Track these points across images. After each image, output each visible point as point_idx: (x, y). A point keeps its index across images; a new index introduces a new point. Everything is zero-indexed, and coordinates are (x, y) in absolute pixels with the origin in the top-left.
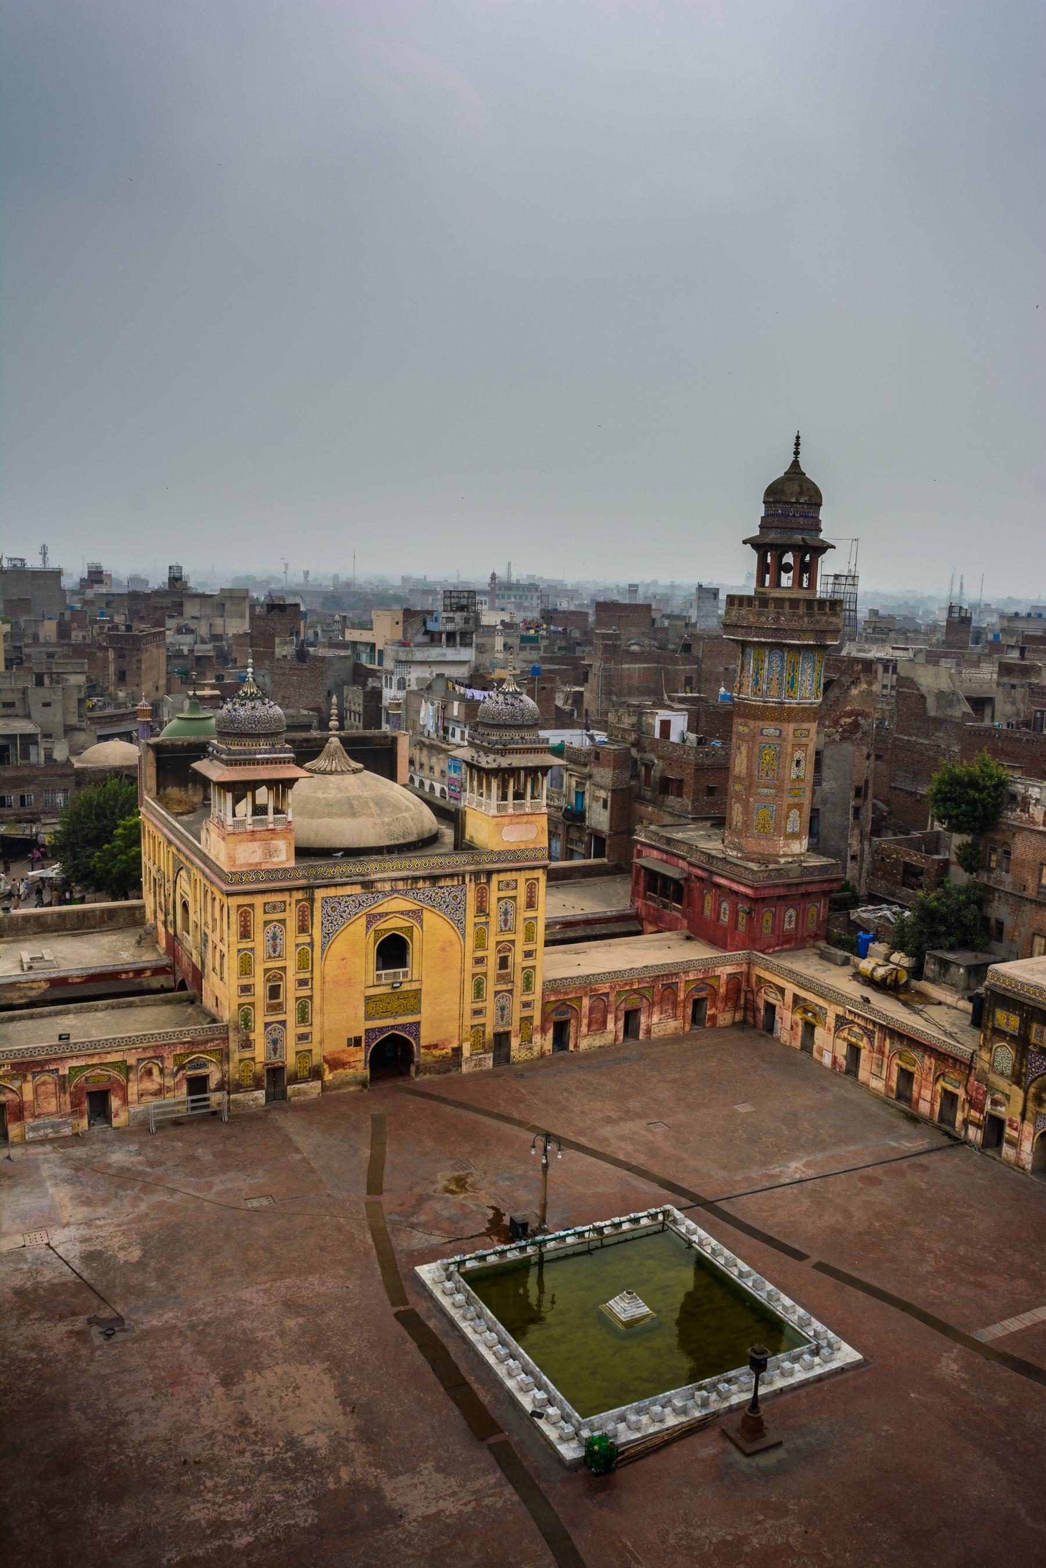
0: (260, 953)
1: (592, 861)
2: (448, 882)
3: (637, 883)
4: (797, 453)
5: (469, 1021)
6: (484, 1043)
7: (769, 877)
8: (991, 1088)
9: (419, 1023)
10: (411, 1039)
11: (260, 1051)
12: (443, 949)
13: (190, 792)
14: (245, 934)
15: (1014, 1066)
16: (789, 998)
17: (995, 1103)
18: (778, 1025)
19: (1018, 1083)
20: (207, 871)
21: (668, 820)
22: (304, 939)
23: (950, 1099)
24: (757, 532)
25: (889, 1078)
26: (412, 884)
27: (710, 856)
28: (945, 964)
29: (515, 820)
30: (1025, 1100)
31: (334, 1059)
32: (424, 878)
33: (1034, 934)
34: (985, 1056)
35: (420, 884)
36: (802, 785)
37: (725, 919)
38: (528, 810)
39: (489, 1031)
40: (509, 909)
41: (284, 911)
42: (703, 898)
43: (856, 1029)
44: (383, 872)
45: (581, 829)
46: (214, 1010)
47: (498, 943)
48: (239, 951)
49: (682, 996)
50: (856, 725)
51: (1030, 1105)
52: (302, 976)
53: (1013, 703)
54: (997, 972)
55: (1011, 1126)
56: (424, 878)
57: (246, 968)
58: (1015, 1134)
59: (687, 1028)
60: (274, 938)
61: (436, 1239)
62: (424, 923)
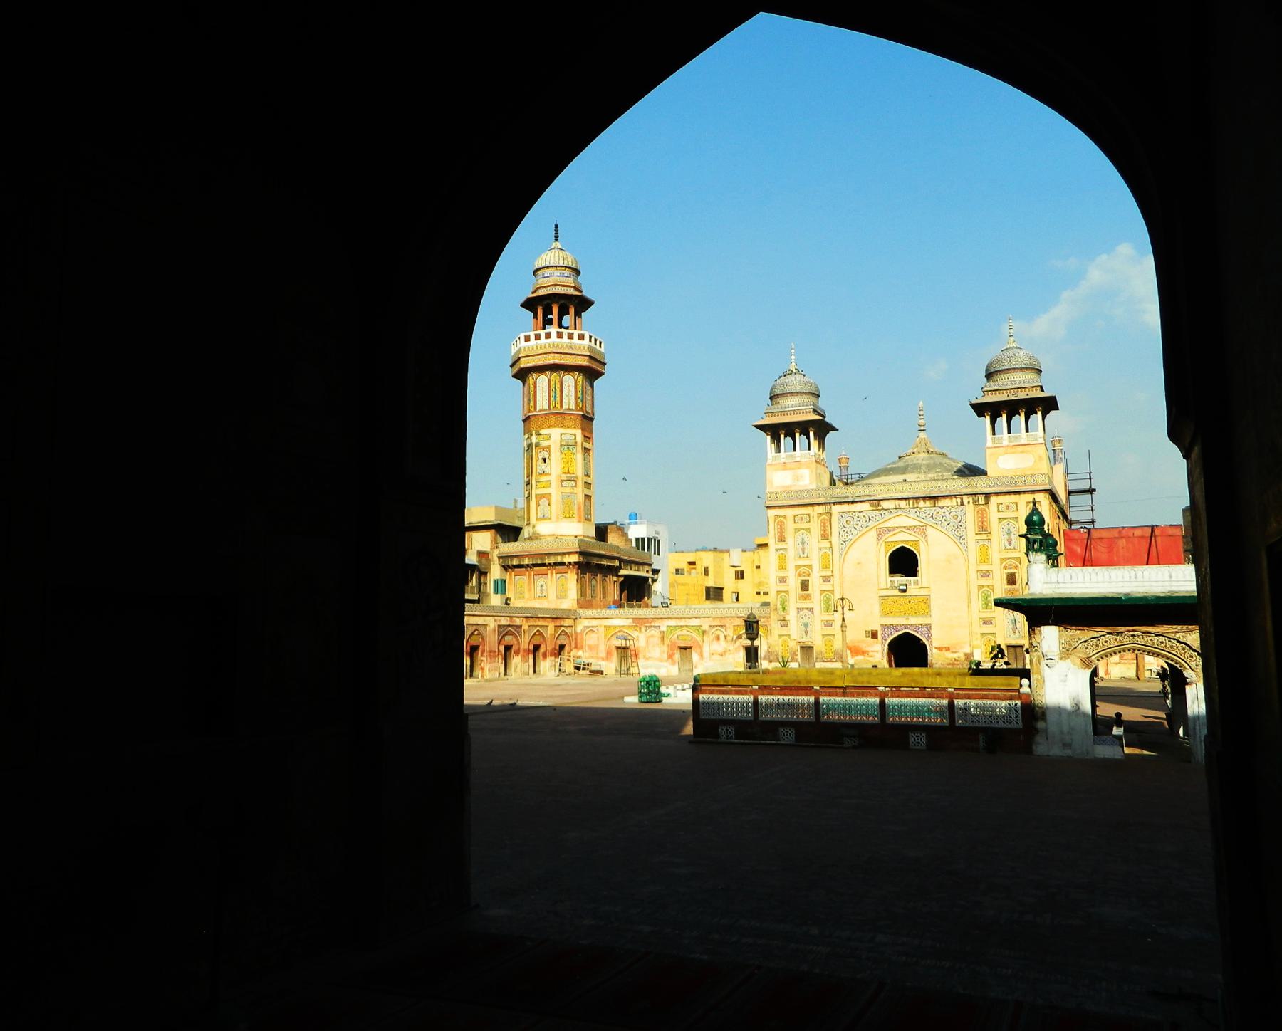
9: (929, 626)
11: (795, 630)
14: (782, 539)
22: (826, 544)
26: (913, 504)
29: (1010, 450)
31: (855, 646)
32: (924, 498)
35: (922, 503)
38: (1023, 442)
40: (1012, 530)
41: (809, 522)
44: (886, 493)
48: (777, 550)
56: (924, 498)
57: (782, 567)
60: (803, 543)
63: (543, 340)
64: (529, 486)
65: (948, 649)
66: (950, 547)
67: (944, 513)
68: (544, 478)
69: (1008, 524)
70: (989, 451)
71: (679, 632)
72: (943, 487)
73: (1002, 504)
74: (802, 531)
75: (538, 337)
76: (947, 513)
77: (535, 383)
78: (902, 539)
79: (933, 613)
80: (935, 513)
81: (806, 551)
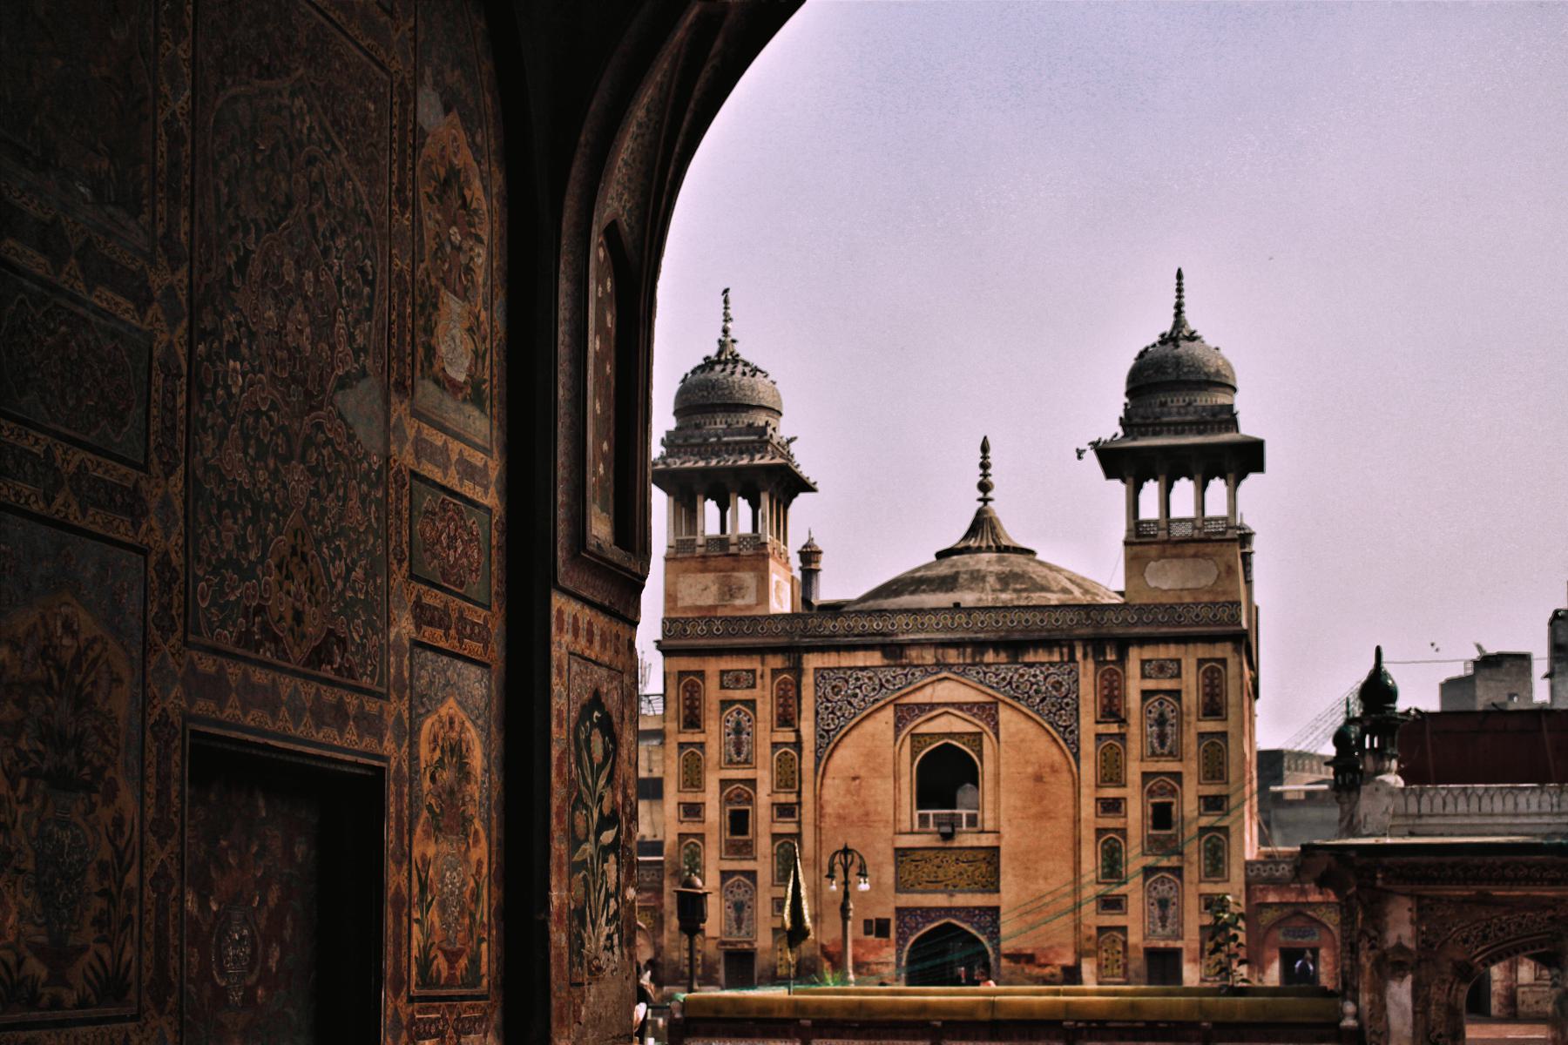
0: (713, 752)
2: (1042, 656)
5: (1092, 918)
6: (1125, 966)
9: (995, 910)
10: (983, 938)
12: (1038, 778)
14: (693, 720)
26: (973, 657)
29: (1170, 550)
32: (997, 646)
35: (990, 657)
44: (918, 631)
48: (681, 746)
52: (782, 798)
57: (693, 777)
62: (1001, 727)
66: (1044, 749)
67: (1035, 676)
69: (1161, 704)
72: (1035, 623)
73: (1150, 661)
74: (737, 706)
76: (1041, 677)
79: (1007, 880)
80: (1016, 677)
81: (745, 750)
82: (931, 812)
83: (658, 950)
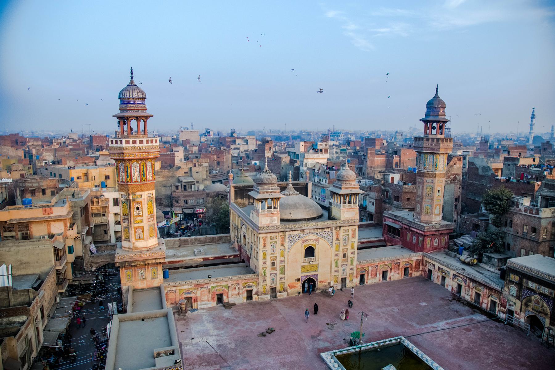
1: (369, 222)
3: (384, 229)
4: (437, 91)
7: (429, 228)
8: (508, 300)
9: (317, 275)
11: (269, 283)
12: (325, 251)
13: (245, 200)
14: (265, 246)
15: (517, 293)
16: (437, 268)
17: (510, 305)
18: (432, 277)
19: (519, 299)
20: (252, 226)
21: (394, 209)
23: (494, 303)
24: (424, 117)
25: (471, 295)
27: (409, 221)
28: (490, 258)
30: (521, 305)
32: (320, 229)
33: (521, 248)
34: (506, 289)
35: (319, 230)
36: (440, 198)
37: (414, 242)
39: (340, 277)
42: (407, 235)
43: (460, 279)
45: (365, 212)
46: (254, 269)
47: (343, 249)
49: (401, 267)
50: (455, 178)
51: (523, 306)
52: (282, 259)
53: (509, 170)
54: (510, 261)
55: (516, 313)
56: (320, 229)
57: (265, 256)
58: (518, 316)
59: (402, 277)
60: (273, 247)
61: (327, 344)
63: (138, 144)
64: (127, 221)
65: (323, 282)
68: (139, 218)
70: (342, 211)
71: (216, 288)
75: (134, 142)
77: (131, 167)
78: (310, 243)
82: (307, 258)
83: (258, 289)
